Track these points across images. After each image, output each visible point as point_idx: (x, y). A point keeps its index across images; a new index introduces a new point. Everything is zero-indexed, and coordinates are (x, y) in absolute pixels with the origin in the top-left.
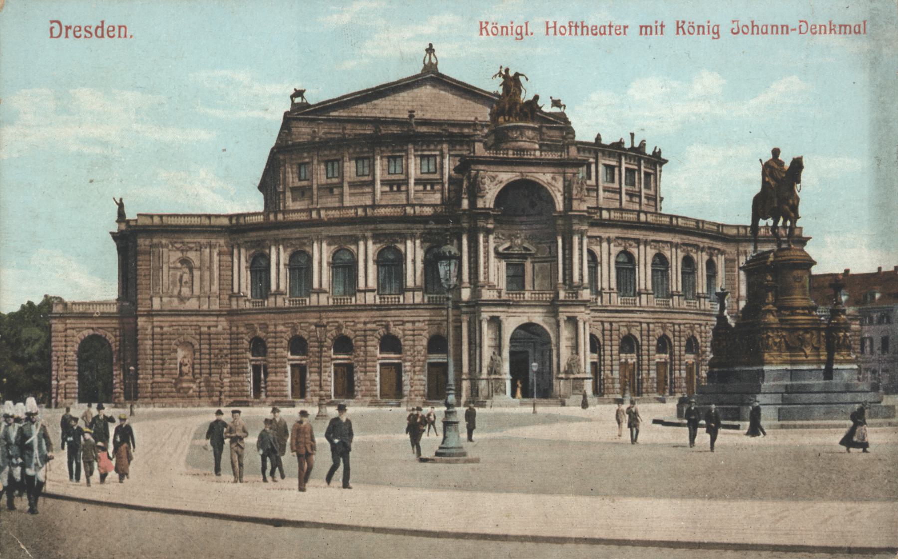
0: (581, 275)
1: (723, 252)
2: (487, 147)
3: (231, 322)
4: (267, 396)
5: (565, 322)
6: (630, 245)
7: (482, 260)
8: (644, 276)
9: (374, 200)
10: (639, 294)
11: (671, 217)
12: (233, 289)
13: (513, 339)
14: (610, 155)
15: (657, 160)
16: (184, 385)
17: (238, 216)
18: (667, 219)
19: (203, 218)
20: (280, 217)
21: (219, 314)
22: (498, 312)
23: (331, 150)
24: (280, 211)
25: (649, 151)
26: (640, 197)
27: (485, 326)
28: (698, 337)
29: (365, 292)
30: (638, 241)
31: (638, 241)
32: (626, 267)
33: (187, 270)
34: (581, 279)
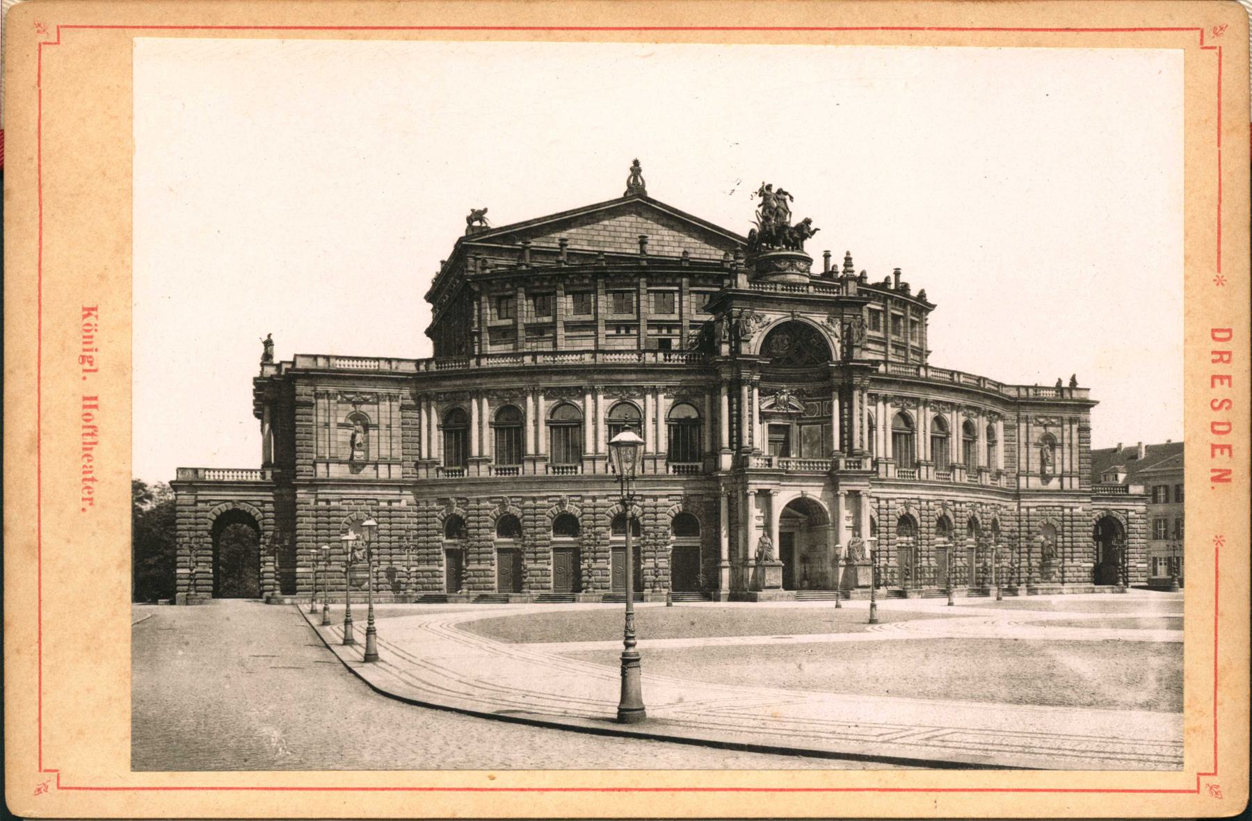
0: (862, 440)
1: (1001, 417)
2: (749, 281)
3: (418, 495)
5: (846, 496)
7: (746, 420)
12: (420, 455)
13: (784, 516)
14: (876, 297)
15: (922, 306)
16: (358, 575)
19: (382, 363)
21: (401, 486)
22: (765, 485)
25: (914, 292)
27: (752, 499)
29: (594, 459)
30: (916, 401)
31: (916, 401)
34: (861, 446)
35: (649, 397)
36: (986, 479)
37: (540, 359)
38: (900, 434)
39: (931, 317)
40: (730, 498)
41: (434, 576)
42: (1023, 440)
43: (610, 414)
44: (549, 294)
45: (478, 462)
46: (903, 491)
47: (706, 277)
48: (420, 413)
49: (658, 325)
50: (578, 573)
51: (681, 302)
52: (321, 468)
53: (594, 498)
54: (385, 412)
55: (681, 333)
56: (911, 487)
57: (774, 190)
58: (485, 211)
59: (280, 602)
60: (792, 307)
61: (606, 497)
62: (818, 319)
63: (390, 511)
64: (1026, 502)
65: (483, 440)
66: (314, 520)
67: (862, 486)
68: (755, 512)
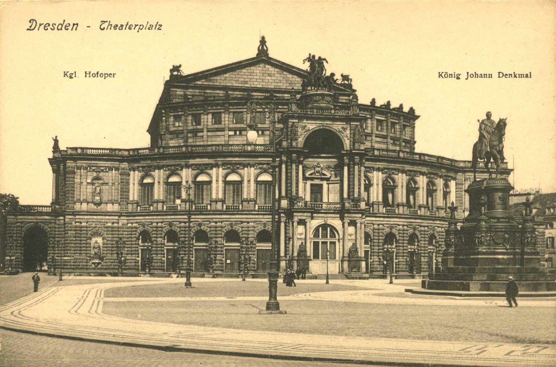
1: (455, 179)
6: (393, 173)
8: (401, 195)
10: (398, 205)
15: (411, 117)
25: (406, 109)
39: (417, 122)
40: (285, 223)
52: (77, 207)
54: (111, 176)
56: (393, 217)
57: (317, 58)
62: (337, 126)
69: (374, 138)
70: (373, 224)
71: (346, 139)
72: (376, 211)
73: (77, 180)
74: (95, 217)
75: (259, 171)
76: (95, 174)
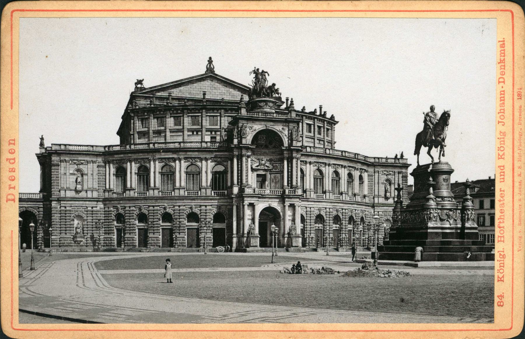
0: (297, 181)
1: (367, 171)
2: (247, 111)
3: (105, 205)
4: (125, 246)
8: (328, 184)
9: (183, 139)
11: (342, 152)
12: (106, 187)
15: (332, 122)
16: (78, 239)
17: (109, 146)
18: (340, 153)
20: (133, 147)
23: (160, 112)
24: (132, 144)
25: (328, 116)
26: (324, 141)
27: (246, 207)
28: (354, 216)
29: (179, 189)
32: (319, 178)
33: (80, 175)
34: (297, 184)
35: (204, 162)
36: (359, 199)
37: (156, 145)
38: (317, 179)
39: (336, 126)
40: (237, 206)
41: (111, 240)
42: (376, 181)
43: (187, 169)
44: (163, 117)
45: (130, 190)
46: (317, 203)
47: (232, 110)
48: (106, 168)
49: (210, 130)
50: (172, 239)
51: (221, 120)
52: (62, 192)
53: (179, 206)
55: (221, 134)
57: (260, 71)
58: (143, 80)
59: (44, 251)
60: (266, 123)
61: (185, 206)
63: (92, 211)
64: (377, 209)
65: (133, 180)
66: (59, 215)
67: (297, 202)
68: (248, 212)
69: (304, 138)
70: (306, 207)
71: (285, 137)
72: (308, 197)
73: (63, 172)
74: (77, 202)
75: (214, 163)
76: (76, 167)
